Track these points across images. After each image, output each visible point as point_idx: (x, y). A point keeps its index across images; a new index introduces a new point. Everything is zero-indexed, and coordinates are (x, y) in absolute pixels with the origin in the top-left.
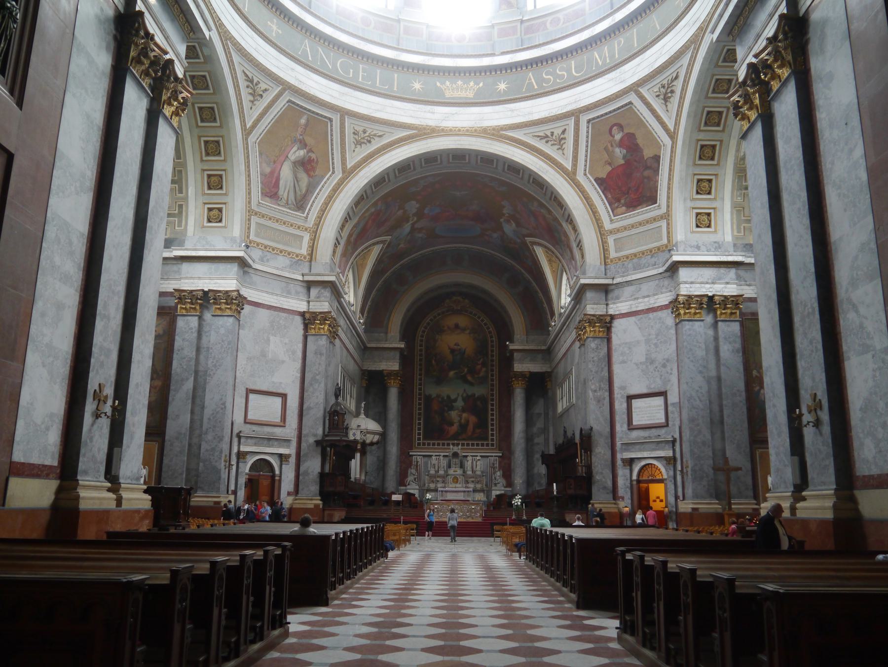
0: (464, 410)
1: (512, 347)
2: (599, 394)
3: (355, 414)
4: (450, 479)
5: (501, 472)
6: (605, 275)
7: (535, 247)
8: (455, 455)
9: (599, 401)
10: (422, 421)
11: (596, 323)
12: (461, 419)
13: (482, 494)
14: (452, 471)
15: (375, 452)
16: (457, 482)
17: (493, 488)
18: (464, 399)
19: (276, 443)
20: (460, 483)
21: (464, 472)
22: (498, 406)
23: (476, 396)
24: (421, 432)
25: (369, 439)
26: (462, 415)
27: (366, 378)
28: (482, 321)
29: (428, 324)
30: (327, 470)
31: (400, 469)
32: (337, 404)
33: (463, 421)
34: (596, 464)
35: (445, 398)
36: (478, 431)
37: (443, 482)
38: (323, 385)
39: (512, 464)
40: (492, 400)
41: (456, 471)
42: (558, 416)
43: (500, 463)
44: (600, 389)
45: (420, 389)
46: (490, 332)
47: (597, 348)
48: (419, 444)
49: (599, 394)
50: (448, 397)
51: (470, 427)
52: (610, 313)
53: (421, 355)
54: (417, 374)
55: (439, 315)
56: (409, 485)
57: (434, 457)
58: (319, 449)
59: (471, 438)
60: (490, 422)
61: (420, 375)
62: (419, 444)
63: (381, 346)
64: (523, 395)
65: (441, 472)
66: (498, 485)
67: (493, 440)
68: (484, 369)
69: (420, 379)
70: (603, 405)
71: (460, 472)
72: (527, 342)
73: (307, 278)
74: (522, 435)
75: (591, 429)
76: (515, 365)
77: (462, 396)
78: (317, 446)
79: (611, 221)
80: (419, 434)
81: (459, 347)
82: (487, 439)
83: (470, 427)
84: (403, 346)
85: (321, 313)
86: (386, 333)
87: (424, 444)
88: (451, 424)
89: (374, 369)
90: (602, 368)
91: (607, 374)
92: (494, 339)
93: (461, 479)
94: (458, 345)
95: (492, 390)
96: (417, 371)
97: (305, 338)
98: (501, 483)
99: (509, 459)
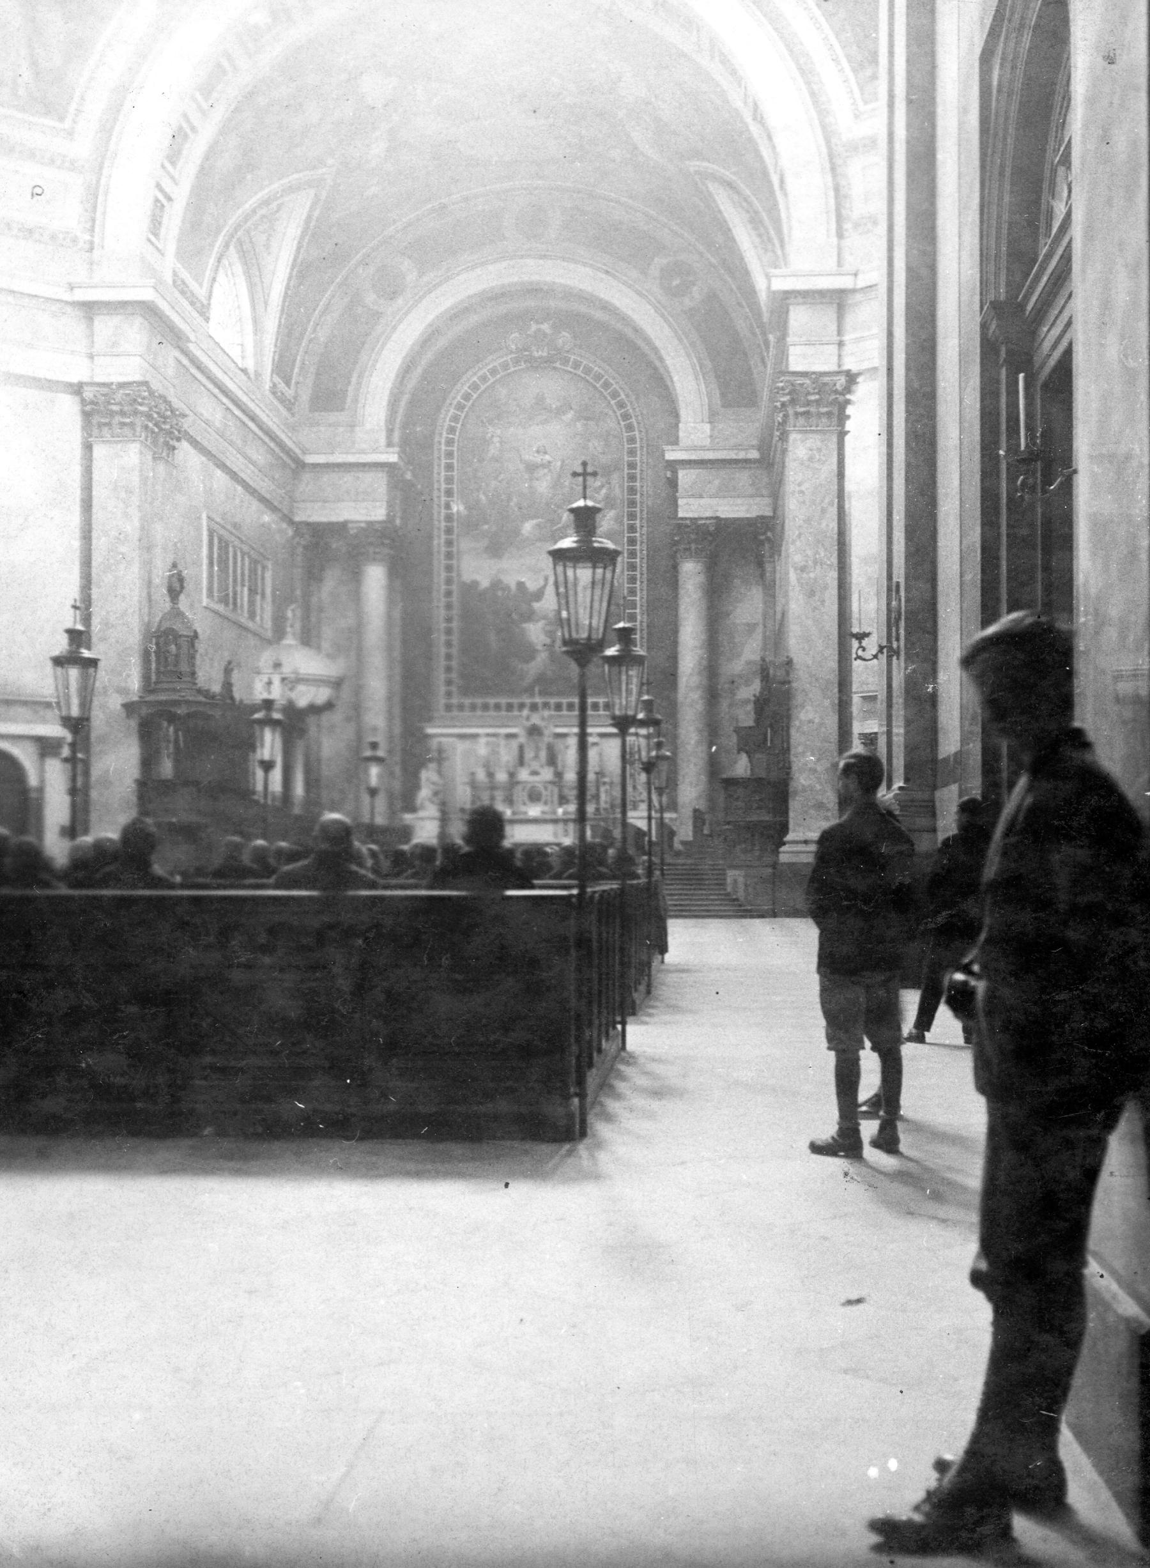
2: (812, 575)
3: (269, 634)
6: (840, 264)
7: (710, 185)
8: (534, 731)
9: (811, 594)
11: (809, 393)
19: (21, 710)
21: (559, 775)
25: (304, 697)
30: (167, 768)
32: (177, 614)
34: (800, 749)
38: (135, 568)
44: (815, 562)
45: (449, 568)
47: (811, 459)
48: (448, 708)
49: (812, 575)
50: (521, 585)
52: (845, 367)
55: (494, 372)
57: (483, 740)
58: (134, 723)
62: (448, 708)
63: (340, 460)
64: (701, 578)
65: (502, 777)
70: (823, 602)
71: (547, 774)
73: (80, 295)
75: (789, 662)
76: (681, 502)
78: (128, 717)
79: (856, 117)
81: (547, 457)
84: (393, 458)
85: (122, 385)
86: (352, 426)
89: (324, 519)
90: (823, 511)
91: (834, 525)
97: (88, 447)
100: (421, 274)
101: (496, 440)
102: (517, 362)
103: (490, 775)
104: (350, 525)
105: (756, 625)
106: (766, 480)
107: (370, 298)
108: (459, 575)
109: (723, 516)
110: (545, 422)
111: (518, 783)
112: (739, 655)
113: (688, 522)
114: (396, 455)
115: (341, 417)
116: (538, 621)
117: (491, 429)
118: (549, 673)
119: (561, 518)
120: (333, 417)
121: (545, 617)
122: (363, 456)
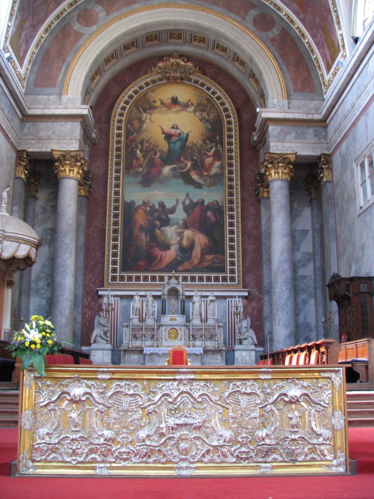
0: (186, 225)
1: (265, 115)
4: (164, 332)
5: (249, 319)
8: (174, 292)
10: (119, 243)
12: (182, 239)
13: (219, 357)
14: (169, 318)
15: (43, 292)
16: (176, 338)
17: (237, 347)
18: (186, 209)
20: (181, 340)
22: (240, 219)
23: (206, 203)
24: (118, 259)
26: (183, 233)
27: (24, 163)
28: (214, 93)
29: (131, 97)
31: (83, 318)
33: (185, 243)
35: (157, 207)
36: (209, 257)
37: (152, 337)
39: (266, 309)
40: (231, 209)
41: (175, 320)
42: (358, 212)
43: (245, 307)
45: (117, 193)
46: (226, 110)
50: (162, 205)
51: (197, 252)
53: (119, 142)
54: (112, 169)
55: (147, 84)
56: (95, 341)
57: (137, 298)
59: (195, 269)
60: (228, 243)
61: (118, 171)
62: (114, 278)
64: (285, 191)
66: (245, 342)
67: (232, 271)
68: (217, 163)
69: (117, 178)
71: (180, 319)
72: (289, 108)
74: (286, 256)
76: (272, 144)
77: (183, 203)
80: (114, 263)
81: (178, 131)
82: (223, 270)
83: (197, 252)
84: (85, 110)
86: (60, 95)
87: (122, 278)
88: (166, 247)
92: (232, 119)
93: (182, 332)
94: (177, 128)
95: (231, 194)
96: (112, 165)
98: (250, 340)
99: (260, 301)
100: (107, 15)
101: (148, 121)
102: (160, 80)
103: (142, 320)
104: (54, 153)
105: (307, 231)
106: (324, 134)
107: (77, 26)
108: (123, 197)
109: (299, 154)
110: (178, 112)
111: (162, 326)
112: (298, 249)
113: (276, 157)
114: (87, 110)
115: (56, 90)
116: (172, 225)
117: (144, 115)
118: (179, 258)
119: (186, 165)
120: (48, 90)
121: (177, 224)
122: (66, 110)
